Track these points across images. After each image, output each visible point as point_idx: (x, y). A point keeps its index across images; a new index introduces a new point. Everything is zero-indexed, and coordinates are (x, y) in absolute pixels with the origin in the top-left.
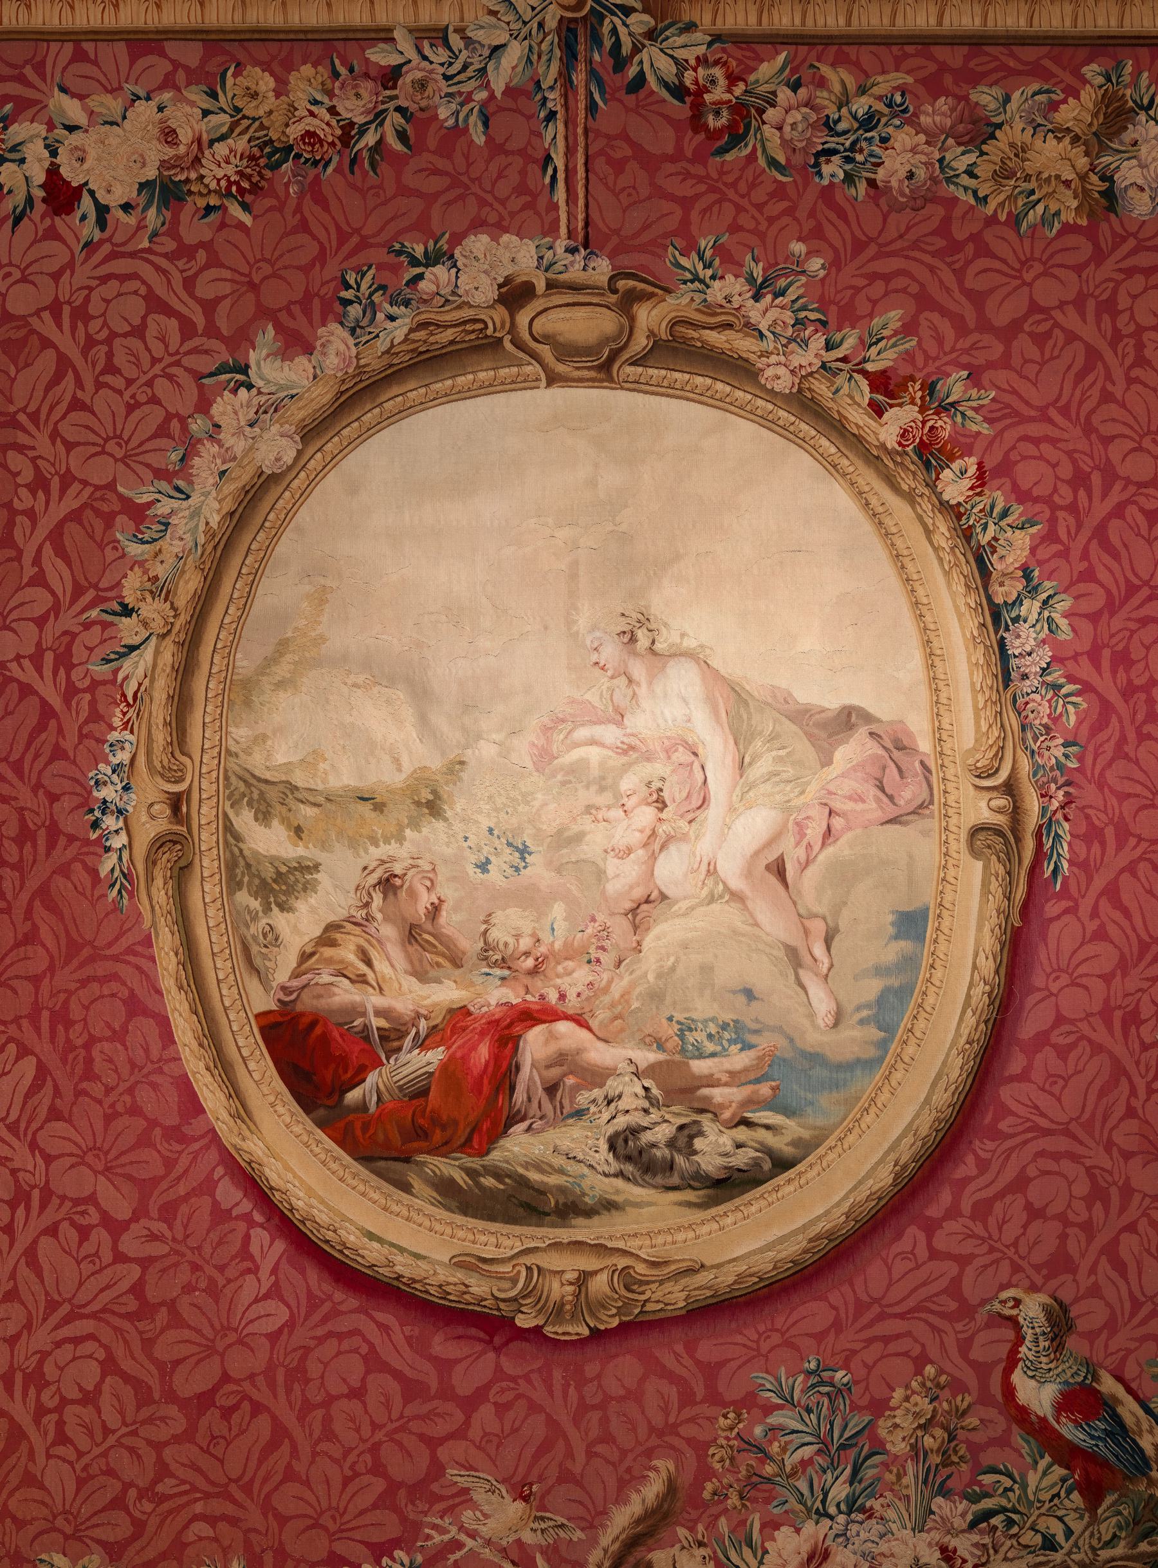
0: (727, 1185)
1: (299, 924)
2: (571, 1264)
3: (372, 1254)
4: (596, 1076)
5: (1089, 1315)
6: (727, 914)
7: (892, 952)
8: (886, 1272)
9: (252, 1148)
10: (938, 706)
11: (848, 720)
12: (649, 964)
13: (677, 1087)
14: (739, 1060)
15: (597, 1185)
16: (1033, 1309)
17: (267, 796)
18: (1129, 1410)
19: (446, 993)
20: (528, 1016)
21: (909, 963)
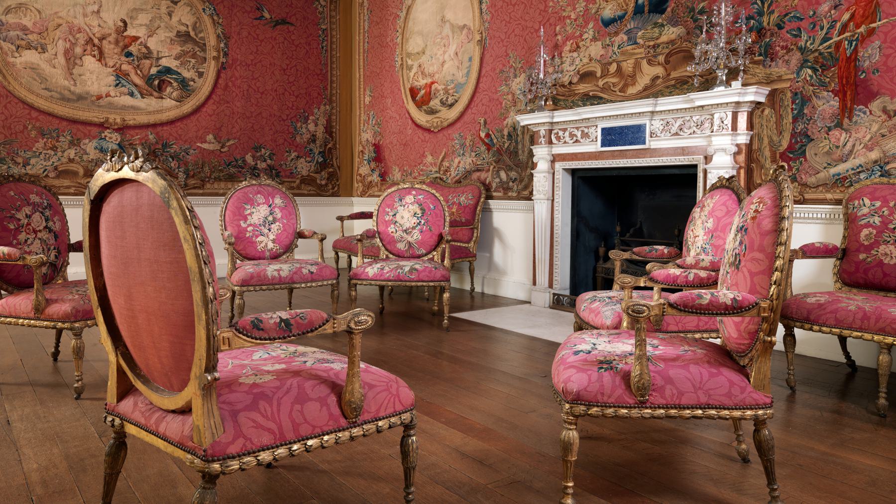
0: (451, 106)
1: (412, 74)
2: (435, 120)
3: (418, 122)
4: (438, 91)
5: (488, 121)
6: (451, 62)
7: (468, 64)
8: (466, 118)
9: (408, 107)
10: (474, 20)
11: (465, 26)
12: (443, 72)
13: (446, 91)
14: (452, 85)
15: (439, 108)
16: (482, 121)
17: (409, 55)
18: (493, 136)
19: (425, 82)
20: (432, 83)
21: (470, 66)
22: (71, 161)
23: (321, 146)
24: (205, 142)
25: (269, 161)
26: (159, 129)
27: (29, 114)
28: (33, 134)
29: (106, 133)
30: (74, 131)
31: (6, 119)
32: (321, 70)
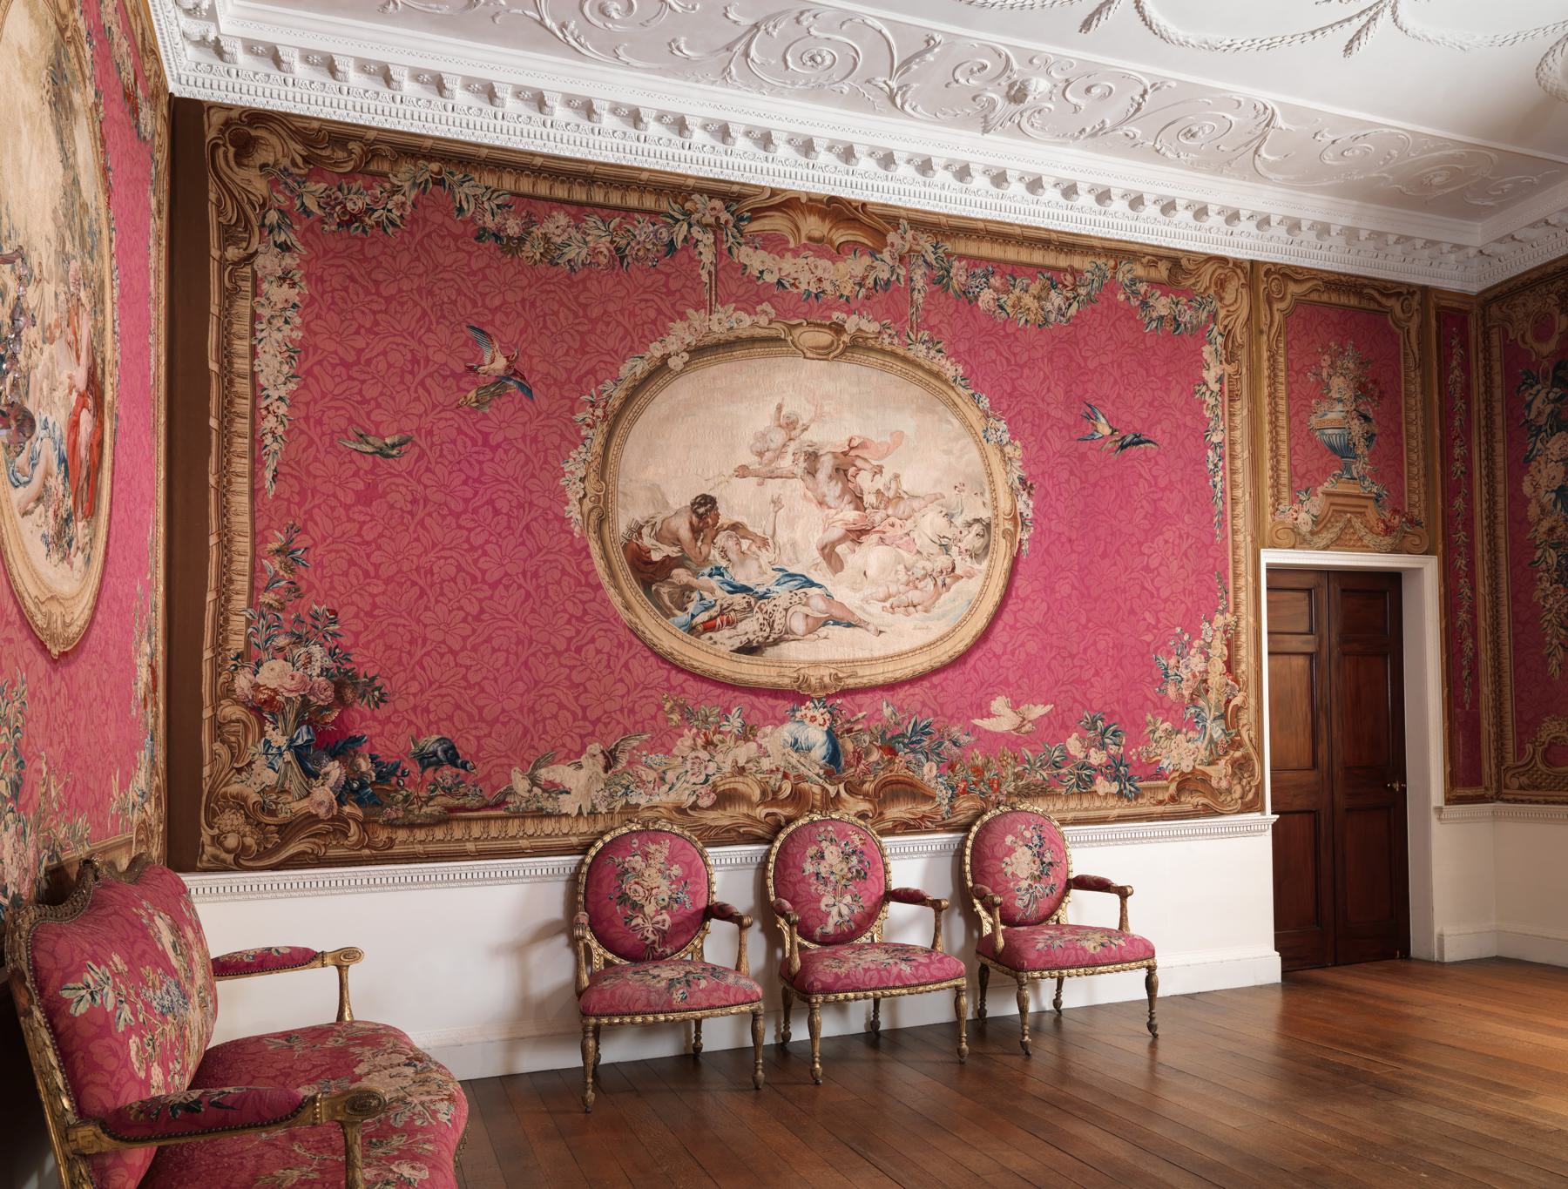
22: (741, 771)
23: (1217, 708)
24: (989, 715)
25: (1113, 749)
26: (902, 693)
27: (668, 679)
28: (676, 717)
29: (808, 710)
30: (747, 709)
31: (628, 693)
32: (1214, 535)
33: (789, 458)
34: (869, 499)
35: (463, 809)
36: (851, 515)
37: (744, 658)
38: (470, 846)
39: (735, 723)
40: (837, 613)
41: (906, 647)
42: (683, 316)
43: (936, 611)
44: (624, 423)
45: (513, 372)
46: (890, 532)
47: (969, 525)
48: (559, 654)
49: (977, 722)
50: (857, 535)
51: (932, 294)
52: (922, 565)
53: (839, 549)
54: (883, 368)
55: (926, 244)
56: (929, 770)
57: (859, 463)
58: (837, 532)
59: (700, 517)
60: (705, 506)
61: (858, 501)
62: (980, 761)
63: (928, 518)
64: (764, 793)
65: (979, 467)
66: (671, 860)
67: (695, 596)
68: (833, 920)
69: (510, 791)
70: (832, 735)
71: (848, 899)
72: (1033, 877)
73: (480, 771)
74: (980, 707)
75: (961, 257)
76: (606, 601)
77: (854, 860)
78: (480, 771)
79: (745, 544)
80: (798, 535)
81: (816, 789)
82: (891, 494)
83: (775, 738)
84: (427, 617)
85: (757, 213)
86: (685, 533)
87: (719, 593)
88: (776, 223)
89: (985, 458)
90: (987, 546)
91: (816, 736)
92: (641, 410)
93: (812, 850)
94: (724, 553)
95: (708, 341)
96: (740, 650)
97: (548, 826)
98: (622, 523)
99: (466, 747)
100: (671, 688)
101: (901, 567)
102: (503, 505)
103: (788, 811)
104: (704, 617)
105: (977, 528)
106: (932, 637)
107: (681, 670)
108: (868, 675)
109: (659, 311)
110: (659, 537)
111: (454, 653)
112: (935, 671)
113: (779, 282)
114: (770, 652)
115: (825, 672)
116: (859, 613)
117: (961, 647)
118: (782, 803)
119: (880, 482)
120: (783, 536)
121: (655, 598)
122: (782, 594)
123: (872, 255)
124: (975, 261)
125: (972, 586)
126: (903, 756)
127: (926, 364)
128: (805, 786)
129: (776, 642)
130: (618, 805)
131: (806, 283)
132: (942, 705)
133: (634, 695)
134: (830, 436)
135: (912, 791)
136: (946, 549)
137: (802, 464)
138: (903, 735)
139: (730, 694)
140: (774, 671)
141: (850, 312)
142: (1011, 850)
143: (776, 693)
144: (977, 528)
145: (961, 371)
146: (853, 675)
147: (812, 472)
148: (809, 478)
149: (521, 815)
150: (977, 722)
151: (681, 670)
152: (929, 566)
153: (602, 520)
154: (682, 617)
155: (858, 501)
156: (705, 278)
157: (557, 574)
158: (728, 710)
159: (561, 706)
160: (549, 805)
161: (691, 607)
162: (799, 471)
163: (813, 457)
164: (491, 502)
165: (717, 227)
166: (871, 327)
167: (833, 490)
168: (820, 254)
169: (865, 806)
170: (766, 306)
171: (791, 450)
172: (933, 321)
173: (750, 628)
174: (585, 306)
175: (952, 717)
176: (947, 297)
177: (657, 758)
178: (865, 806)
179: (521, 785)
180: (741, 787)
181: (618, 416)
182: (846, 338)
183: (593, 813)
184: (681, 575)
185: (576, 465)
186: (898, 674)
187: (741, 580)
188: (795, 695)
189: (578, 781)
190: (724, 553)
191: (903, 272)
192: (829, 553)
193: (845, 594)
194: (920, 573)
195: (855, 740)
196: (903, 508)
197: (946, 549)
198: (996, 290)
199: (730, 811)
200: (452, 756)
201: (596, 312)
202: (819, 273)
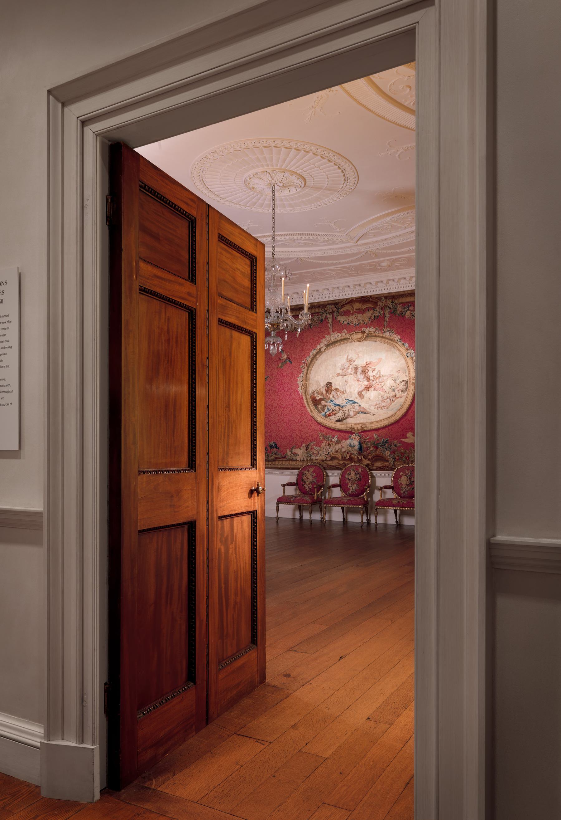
22: (337, 452)
24: (406, 438)
26: (380, 431)
28: (322, 438)
29: (354, 436)
33: (350, 370)
34: (371, 378)
35: (278, 458)
36: (366, 383)
37: (338, 423)
38: (279, 466)
39: (335, 439)
40: (362, 410)
41: (381, 419)
42: (324, 337)
43: (390, 408)
44: (311, 366)
45: (288, 358)
46: (377, 387)
47: (401, 382)
48: (297, 423)
49: (402, 440)
50: (368, 388)
51: (391, 317)
52: (386, 395)
53: (363, 393)
54: (376, 341)
55: (389, 302)
56: (387, 453)
57: (369, 368)
58: (363, 388)
59: (328, 388)
60: (329, 384)
61: (368, 379)
62: (403, 451)
63: (389, 381)
64: (342, 457)
65: (405, 365)
66: (313, 472)
67: (326, 407)
68: (351, 490)
69: (287, 454)
70: (359, 442)
71: (355, 485)
72: (407, 485)
73: (281, 450)
74: (403, 435)
75: (400, 304)
76: (306, 410)
77: (358, 476)
78: (281, 450)
79: (339, 393)
80: (352, 390)
81: (356, 457)
82: (378, 376)
83: (346, 443)
84: (272, 416)
85: (342, 306)
86: (324, 392)
87: (332, 406)
88: (348, 307)
89: (407, 362)
90: (407, 388)
91: (356, 443)
92: (315, 362)
93: (348, 472)
94: (333, 396)
95: (330, 342)
96: (337, 421)
97: (294, 463)
98: (310, 391)
99: (279, 444)
100: (321, 431)
101: (380, 396)
102: (286, 389)
103: (348, 462)
104: (328, 413)
105: (403, 383)
106: (389, 415)
107: (323, 426)
108: (370, 427)
109: (319, 337)
110: (318, 394)
111: (276, 423)
112: (390, 425)
113: (348, 323)
114: (344, 421)
115: (358, 426)
116: (368, 410)
117: (398, 418)
118: (347, 460)
119: (374, 373)
120: (348, 391)
121: (317, 409)
122: (348, 406)
123: (374, 310)
124: (404, 304)
125: (402, 400)
126: (380, 449)
127: (389, 337)
128: (353, 456)
129: (346, 418)
130: (309, 459)
131: (355, 322)
132: (391, 435)
133: (312, 433)
134: (360, 362)
135: (381, 458)
136: (394, 390)
137: (353, 371)
138: (380, 443)
139: (334, 432)
140: (345, 426)
141: (367, 327)
142: (401, 476)
143: (346, 432)
144: (403, 383)
145: (399, 337)
146: (366, 427)
147: (356, 373)
148: (355, 374)
149: (289, 460)
150: (402, 440)
151: (323, 426)
152: (388, 395)
153: (306, 391)
154: (323, 413)
155: (368, 379)
156: (330, 326)
157: (296, 404)
158: (334, 436)
159: (297, 435)
160: (294, 458)
161: (326, 411)
162: (352, 373)
163: (356, 368)
164: (283, 389)
165: (333, 313)
166: (372, 330)
167: (361, 377)
168: (359, 313)
169: (368, 462)
170: (345, 330)
171: (350, 367)
172: (391, 324)
173: (339, 415)
174: (302, 340)
175: (394, 438)
176: (396, 316)
177: (317, 448)
178: (368, 462)
179: (289, 453)
180: (337, 456)
181: (309, 365)
182: (366, 335)
183: (303, 460)
184: (323, 403)
185: (300, 378)
186: (379, 426)
187: (337, 403)
188: (349, 433)
189: (300, 452)
190: (333, 396)
191: (382, 312)
192: (360, 394)
193: (364, 405)
194: (386, 398)
195: (366, 444)
196: (381, 380)
197: (394, 390)
198: (411, 311)
199: (334, 462)
200: (276, 446)
201: (305, 340)
202: (359, 318)
